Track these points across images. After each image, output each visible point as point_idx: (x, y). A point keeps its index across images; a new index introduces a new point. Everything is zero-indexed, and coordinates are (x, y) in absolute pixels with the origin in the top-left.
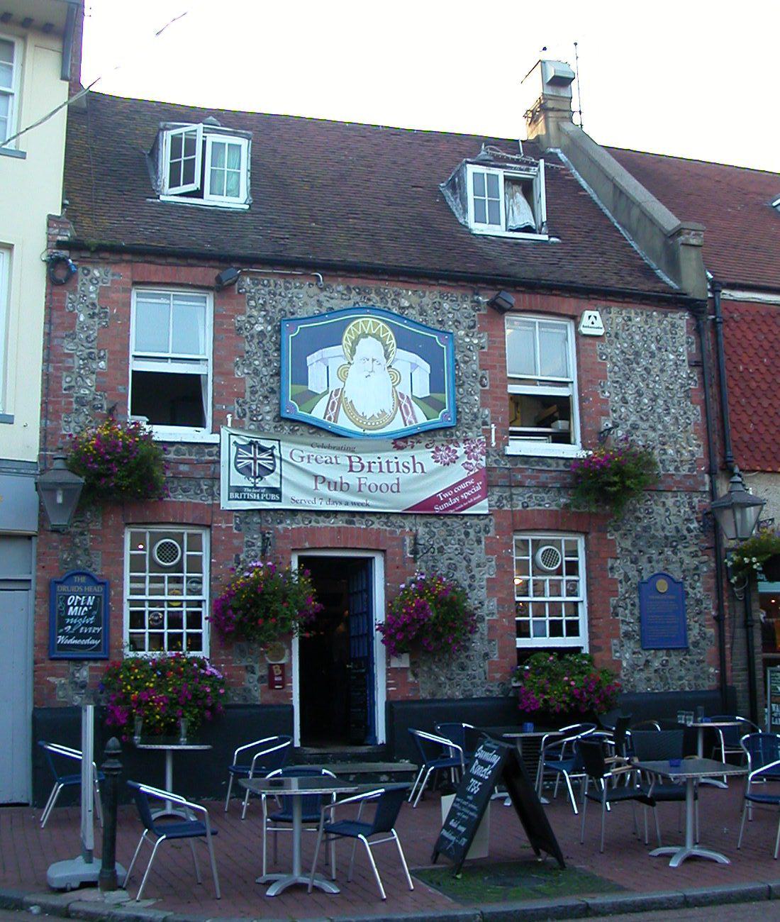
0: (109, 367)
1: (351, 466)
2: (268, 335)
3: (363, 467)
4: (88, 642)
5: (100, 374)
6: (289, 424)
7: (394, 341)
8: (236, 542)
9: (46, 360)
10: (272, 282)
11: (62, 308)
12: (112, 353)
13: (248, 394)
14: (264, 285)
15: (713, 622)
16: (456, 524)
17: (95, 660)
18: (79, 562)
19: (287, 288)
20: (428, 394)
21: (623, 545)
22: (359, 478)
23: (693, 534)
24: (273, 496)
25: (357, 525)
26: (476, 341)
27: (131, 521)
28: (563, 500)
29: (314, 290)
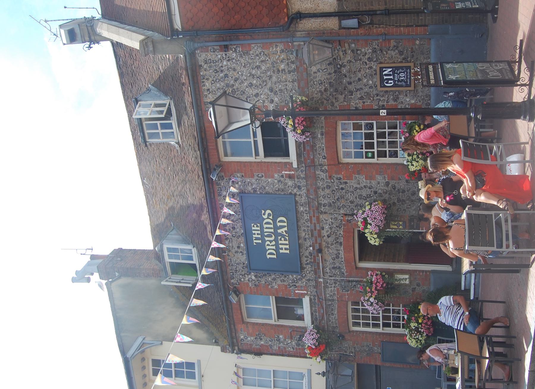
0: (282, 334)
2: (256, 274)
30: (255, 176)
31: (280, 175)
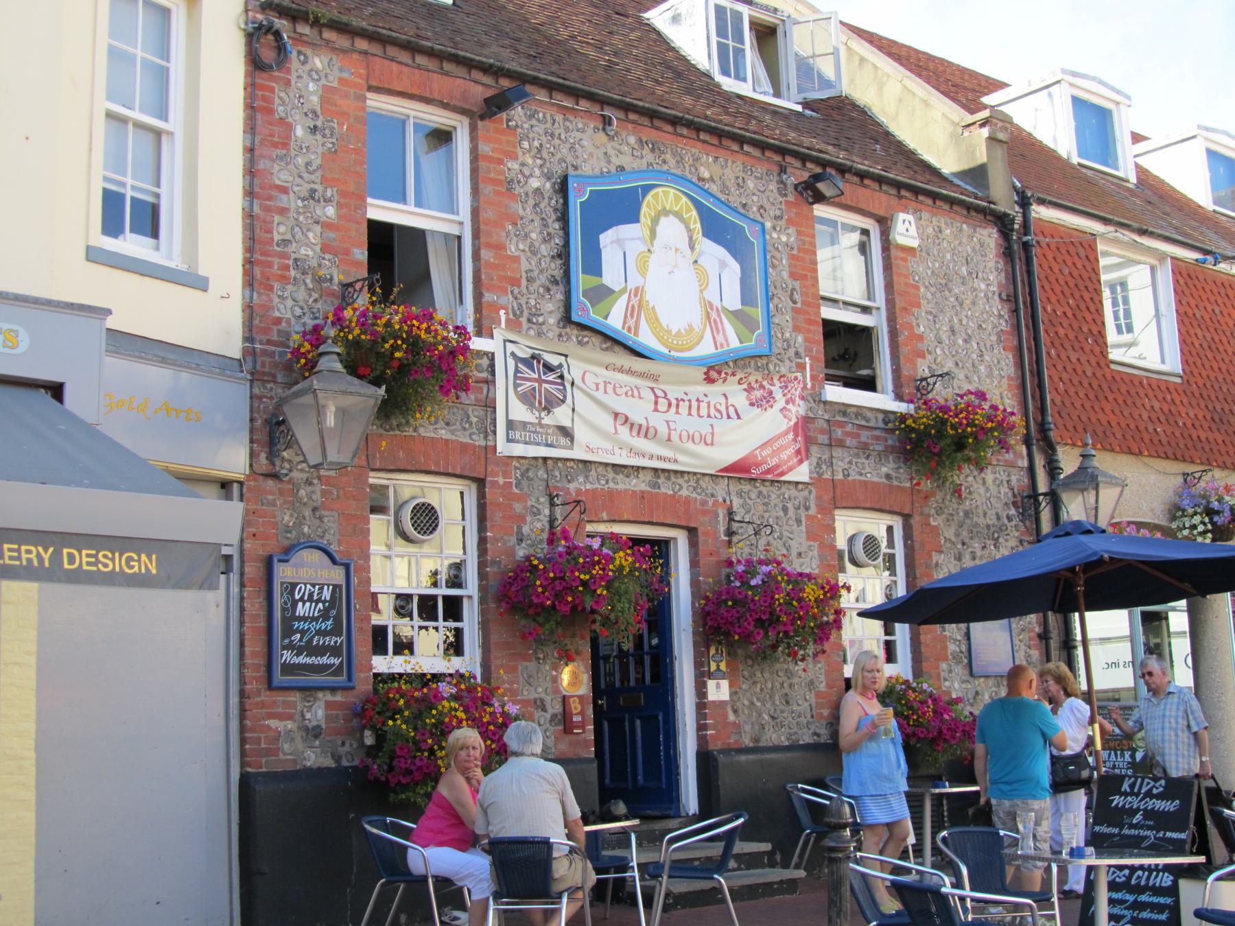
0: (339, 216)
1: (656, 403)
2: (546, 195)
3: (670, 405)
4: (324, 660)
5: (327, 226)
6: (575, 332)
7: (698, 225)
8: (518, 507)
9: (250, 193)
10: (548, 117)
11: (270, 111)
12: (343, 194)
13: (524, 282)
14: (538, 120)
15: (1037, 641)
16: (774, 494)
17: (333, 689)
18: (306, 529)
19: (567, 130)
20: (738, 306)
21: (946, 534)
22: (667, 422)
23: (1013, 523)
24: (563, 441)
25: (663, 490)
26: (784, 239)
27: (378, 466)
28: (884, 470)
29: (601, 136)
30: (794, 283)
31: (801, 350)
